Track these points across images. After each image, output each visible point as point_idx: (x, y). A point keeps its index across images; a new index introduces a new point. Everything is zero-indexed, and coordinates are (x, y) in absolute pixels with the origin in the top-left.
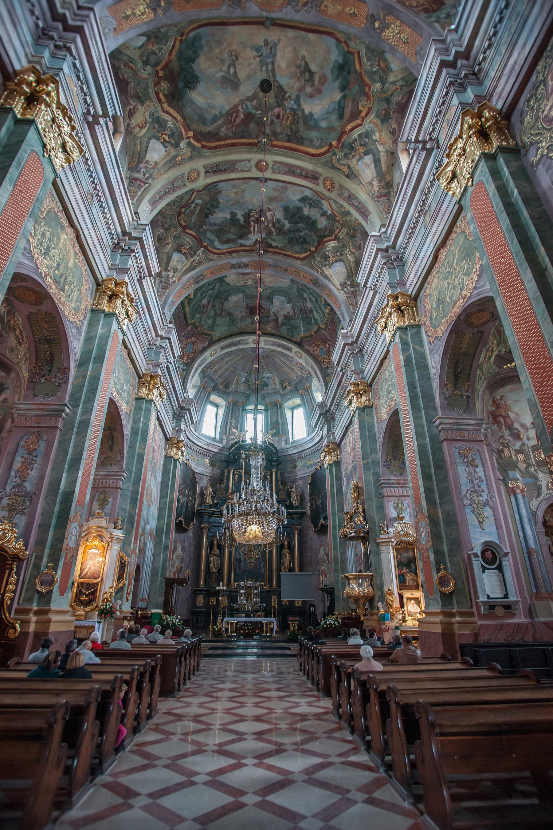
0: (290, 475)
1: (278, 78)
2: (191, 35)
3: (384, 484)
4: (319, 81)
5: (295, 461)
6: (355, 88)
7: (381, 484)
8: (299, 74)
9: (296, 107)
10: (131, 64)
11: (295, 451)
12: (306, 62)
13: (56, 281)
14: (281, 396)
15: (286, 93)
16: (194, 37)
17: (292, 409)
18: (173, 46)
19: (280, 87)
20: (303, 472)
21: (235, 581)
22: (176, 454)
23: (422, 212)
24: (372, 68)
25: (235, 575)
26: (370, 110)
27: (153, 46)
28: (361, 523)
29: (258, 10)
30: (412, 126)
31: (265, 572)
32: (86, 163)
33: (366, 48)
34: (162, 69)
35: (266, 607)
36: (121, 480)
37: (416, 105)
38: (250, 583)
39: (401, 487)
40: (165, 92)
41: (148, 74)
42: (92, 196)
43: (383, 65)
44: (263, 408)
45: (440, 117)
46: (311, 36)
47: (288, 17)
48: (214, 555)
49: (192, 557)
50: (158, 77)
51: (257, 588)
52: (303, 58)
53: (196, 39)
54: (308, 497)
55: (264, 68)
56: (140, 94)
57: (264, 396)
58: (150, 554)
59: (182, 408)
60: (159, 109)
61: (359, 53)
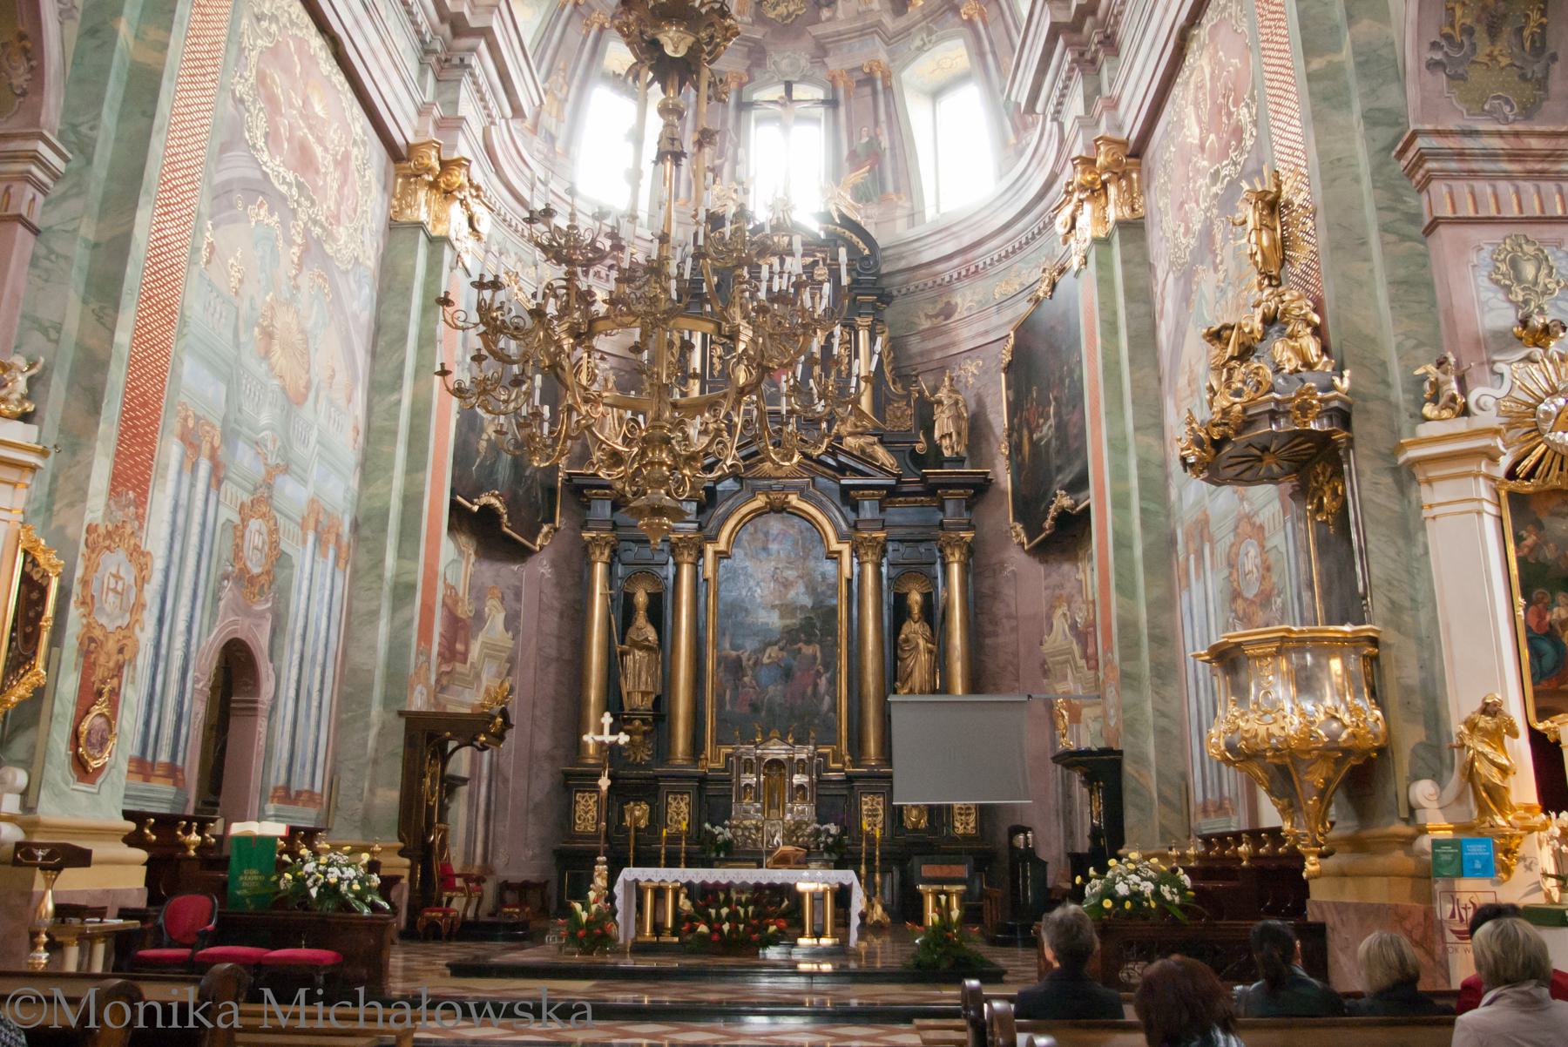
0: (930, 345)
3: (1437, 155)
5: (945, 287)
7: (1422, 157)
11: (949, 248)
14: (890, 40)
17: (936, 94)
20: (979, 327)
21: (719, 742)
22: (438, 219)
25: (721, 720)
28: (1309, 365)
31: (834, 707)
35: (838, 840)
36: (27, 178)
38: (777, 750)
39: (1530, 175)
44: (820, 94)
48: (637, 645)
49: (553, 653)
51: (802, 766)
54: (999, 419)
57: (821, 51)
58: (319, 611)
59: (458, 26)
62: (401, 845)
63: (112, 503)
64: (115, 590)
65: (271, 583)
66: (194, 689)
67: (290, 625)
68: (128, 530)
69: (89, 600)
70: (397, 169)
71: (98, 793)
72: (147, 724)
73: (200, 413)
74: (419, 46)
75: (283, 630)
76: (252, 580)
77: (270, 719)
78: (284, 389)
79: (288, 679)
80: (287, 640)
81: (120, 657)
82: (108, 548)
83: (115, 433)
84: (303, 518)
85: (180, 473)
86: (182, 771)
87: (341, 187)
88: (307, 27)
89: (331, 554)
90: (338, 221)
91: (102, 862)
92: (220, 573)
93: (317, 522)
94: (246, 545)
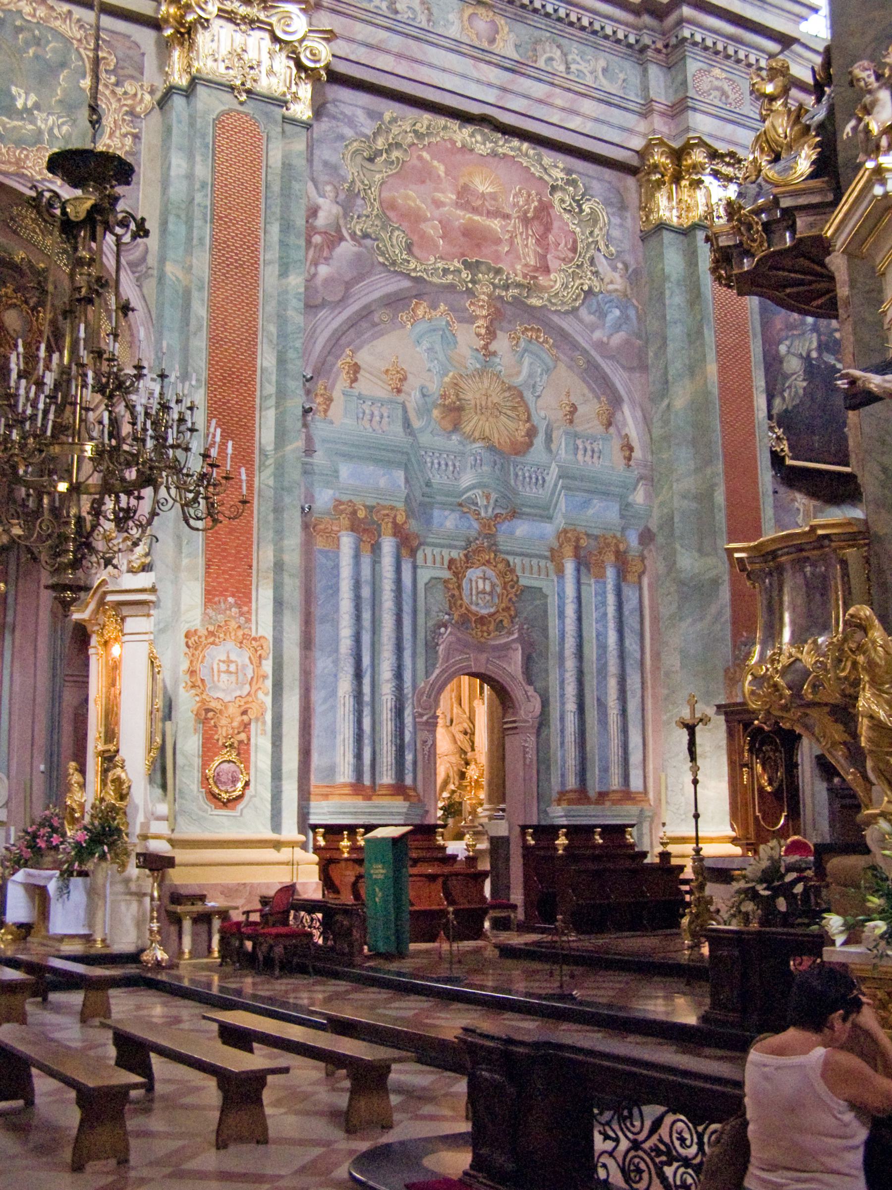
62: (733, 834)
63: (210, 611)
64: (228, 672)
65: (512, 618)
66: (415, 724)
67: (554, 648)
68: (233, 624)
69: (199, 683)
70: (638, 181)
71: (241, 815)
72: (359, 756)
73: (371, 502)
74: (629, 51)
75: (544, 655)
76: (482, 620)
77: (538, 734)
78: (491, 448)
79: (562, 696)
80: (552, 662)
81: (245, 718)
82: (213, 643)
83: (201, 561)
84: (552, 550)
85: (357, 557)
86: (415, 789)
87: (542, 240)
88: (445, 128)
89: (610, 574)
90: (547, 270)
91: (181, 865)
92: (430, 624)
93: (577, 548)
94: (465, 593)
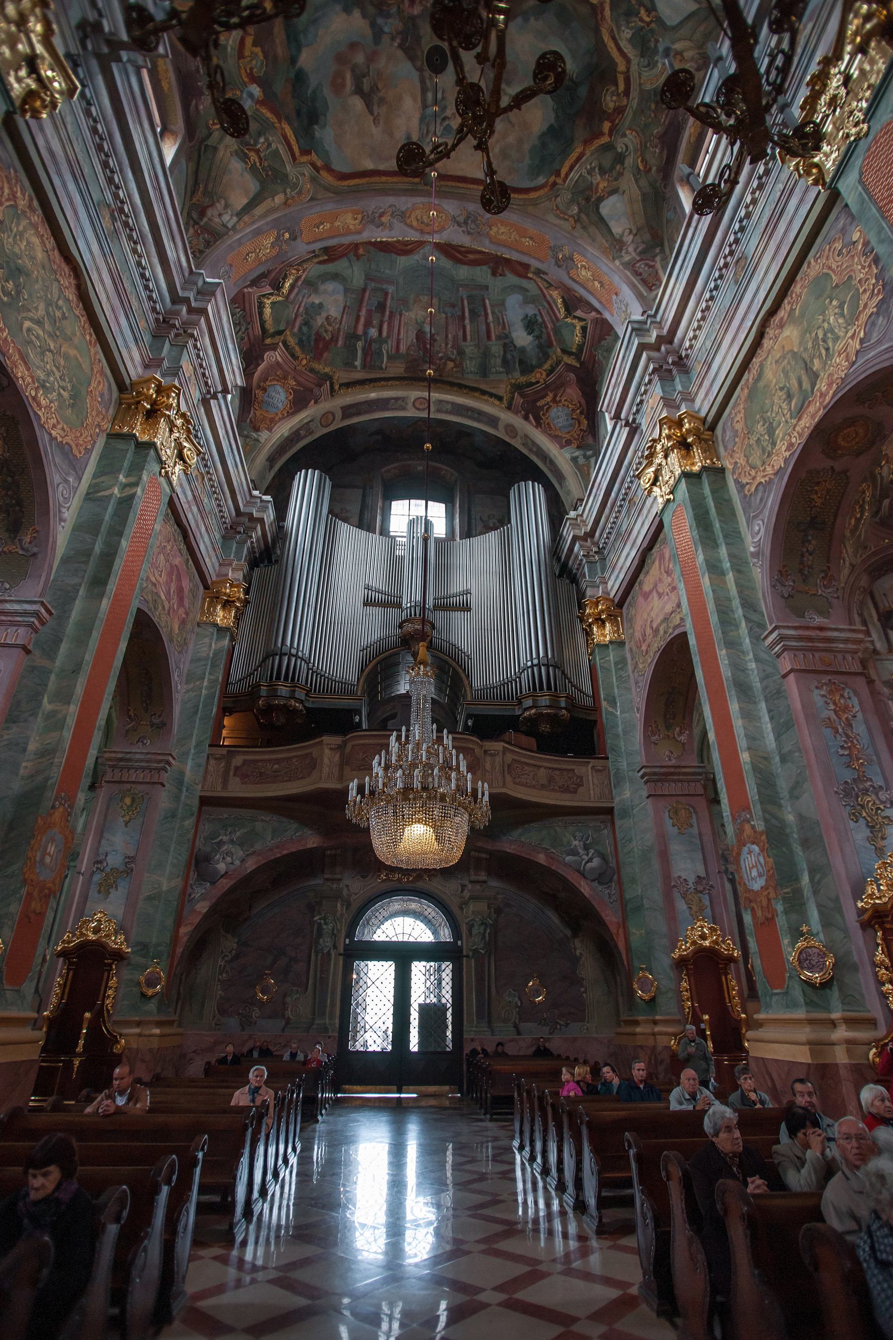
1: (416, 75)
2: (541, 180)
4: (344, 79)
6: (280, 87)
8: (380, 86)
9: (380, 21)
10: (641, 168)
12: (372, 113)
13: (799, 413)
15: (400, 46)
16: (538, 175)
18: (571, 168)
19: (412, 59)
23: (118, 211)
24: (267, 140)
26: (241, 55)
27: (598, 184)
29: (444, 205)
30: (219, 312)
32: (708, 308)
33: (286, 176)
34: (602, 134)
37: (227, 333)
40: (613, 88)
41: (624, 135)
42: (737, 261)
43: (253, 156)
45: (200, 371)
46: (369, 165)
47: (403, 199)
50: (612, 122)
52: (376, 121)
53: (535, 171)
55: (439, 96)
56: (653, 106)
60: (634, 68)
61: (294, 158)
